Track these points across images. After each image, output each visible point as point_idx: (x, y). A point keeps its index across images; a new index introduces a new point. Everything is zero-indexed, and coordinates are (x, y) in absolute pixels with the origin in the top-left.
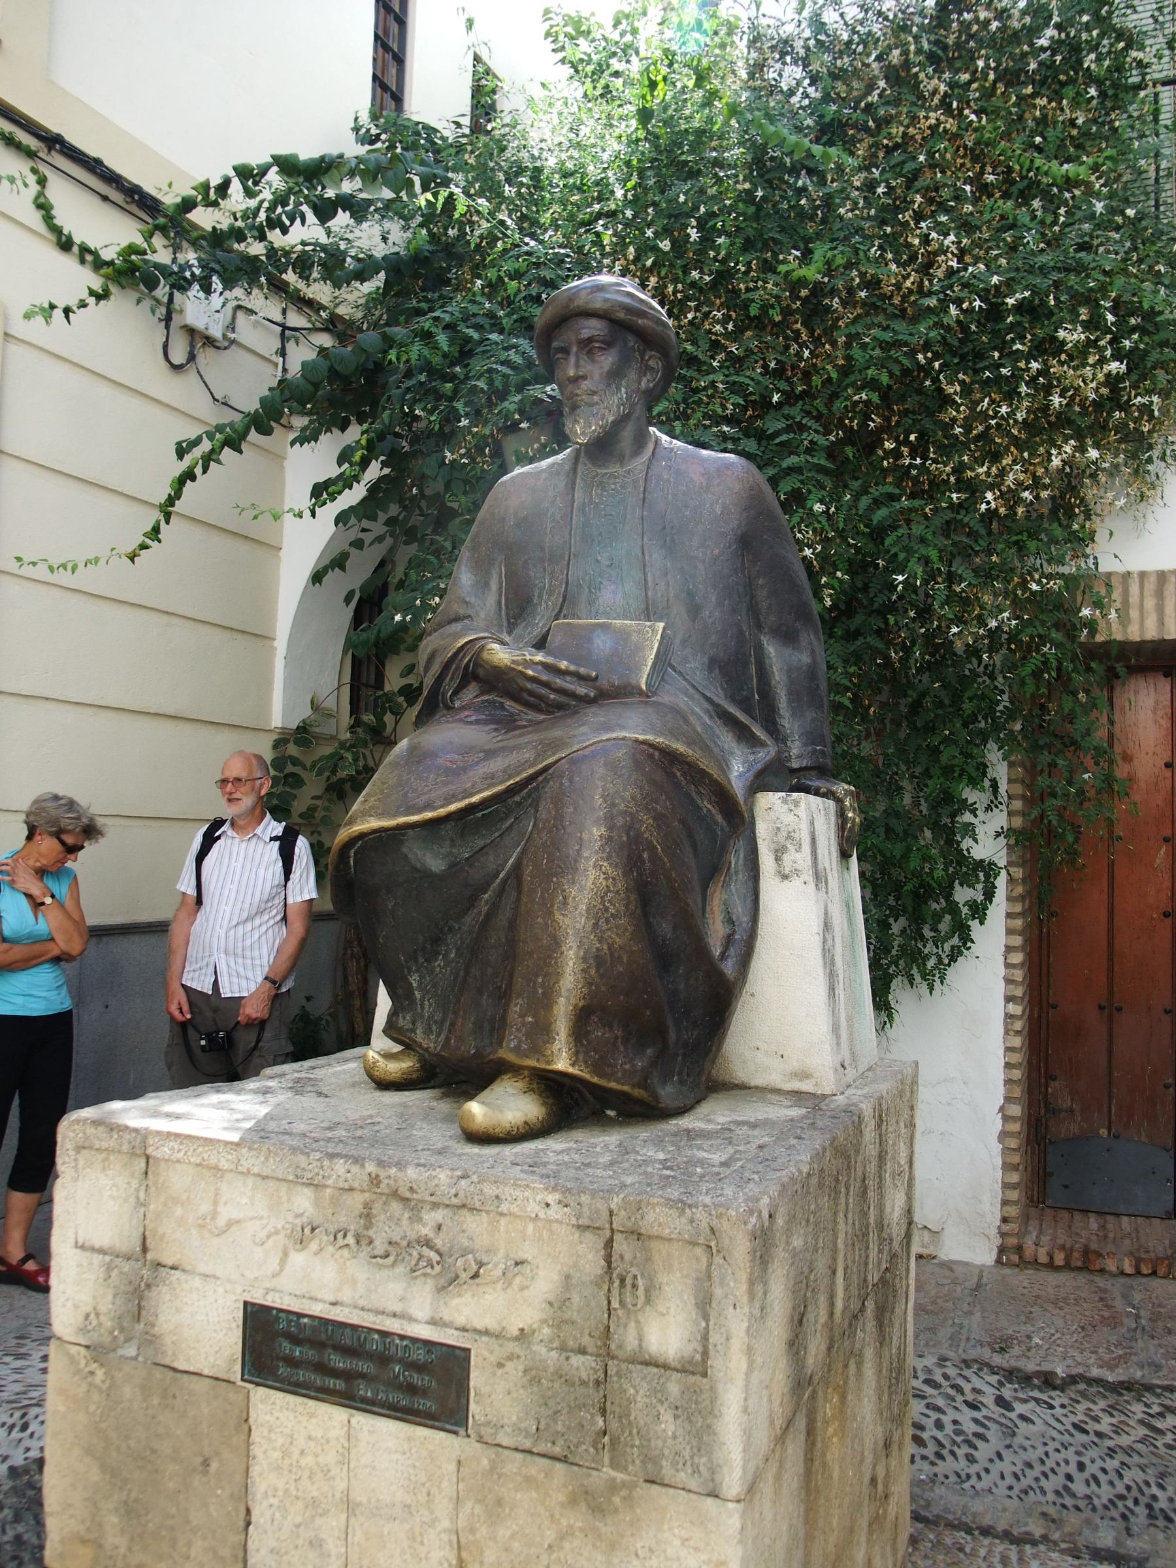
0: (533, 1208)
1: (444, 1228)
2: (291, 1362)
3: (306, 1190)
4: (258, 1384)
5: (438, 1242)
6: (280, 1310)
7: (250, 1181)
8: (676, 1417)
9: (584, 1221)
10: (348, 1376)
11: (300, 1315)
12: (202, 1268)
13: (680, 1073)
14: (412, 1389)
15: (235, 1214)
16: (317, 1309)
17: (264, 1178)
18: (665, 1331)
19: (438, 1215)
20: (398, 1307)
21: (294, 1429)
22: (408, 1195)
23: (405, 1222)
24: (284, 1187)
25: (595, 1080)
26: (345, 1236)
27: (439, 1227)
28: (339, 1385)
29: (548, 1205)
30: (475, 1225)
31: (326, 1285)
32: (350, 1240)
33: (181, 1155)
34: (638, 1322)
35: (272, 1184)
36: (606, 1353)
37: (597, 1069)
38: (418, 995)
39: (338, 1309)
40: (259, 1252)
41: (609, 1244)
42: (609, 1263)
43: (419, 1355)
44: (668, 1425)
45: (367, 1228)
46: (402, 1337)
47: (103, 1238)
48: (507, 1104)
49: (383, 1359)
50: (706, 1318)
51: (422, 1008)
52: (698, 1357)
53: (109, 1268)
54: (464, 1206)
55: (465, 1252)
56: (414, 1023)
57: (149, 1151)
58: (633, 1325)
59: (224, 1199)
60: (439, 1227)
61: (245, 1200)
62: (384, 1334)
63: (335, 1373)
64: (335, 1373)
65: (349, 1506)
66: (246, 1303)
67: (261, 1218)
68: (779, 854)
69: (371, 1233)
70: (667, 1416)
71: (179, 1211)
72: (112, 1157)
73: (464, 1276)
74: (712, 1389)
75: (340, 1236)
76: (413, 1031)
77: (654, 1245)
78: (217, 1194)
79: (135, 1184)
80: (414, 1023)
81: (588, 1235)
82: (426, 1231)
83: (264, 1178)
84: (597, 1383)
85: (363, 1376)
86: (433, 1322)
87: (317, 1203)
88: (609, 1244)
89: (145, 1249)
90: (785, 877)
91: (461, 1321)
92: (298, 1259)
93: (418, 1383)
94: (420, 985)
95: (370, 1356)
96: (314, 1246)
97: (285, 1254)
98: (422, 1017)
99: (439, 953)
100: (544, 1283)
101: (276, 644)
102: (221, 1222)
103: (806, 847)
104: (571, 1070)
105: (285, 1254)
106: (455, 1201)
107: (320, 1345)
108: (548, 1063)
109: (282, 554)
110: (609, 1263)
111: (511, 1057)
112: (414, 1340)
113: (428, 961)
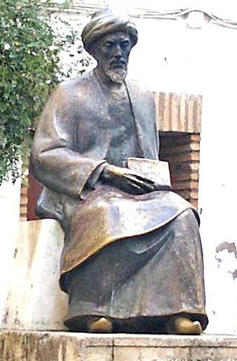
3: (170, 349)
5: (212, 358)
7: (152, 349)
17: (156, 347)
19: (212, 350)
22: (203, 345)
24: (163, 349)
33: (127, 344)
38: (113, 298)
51: (114, 301)
57: (115, 344)
59: (143, 355)
60: (212, 354)
61: (150, 355)
78: (141, 354)
80: (108, 310)
82: (208, 355)
83: (156, 347)
87: (174, 352)
98: (113, 306)
99: (125, 282)
113: (122, 284)
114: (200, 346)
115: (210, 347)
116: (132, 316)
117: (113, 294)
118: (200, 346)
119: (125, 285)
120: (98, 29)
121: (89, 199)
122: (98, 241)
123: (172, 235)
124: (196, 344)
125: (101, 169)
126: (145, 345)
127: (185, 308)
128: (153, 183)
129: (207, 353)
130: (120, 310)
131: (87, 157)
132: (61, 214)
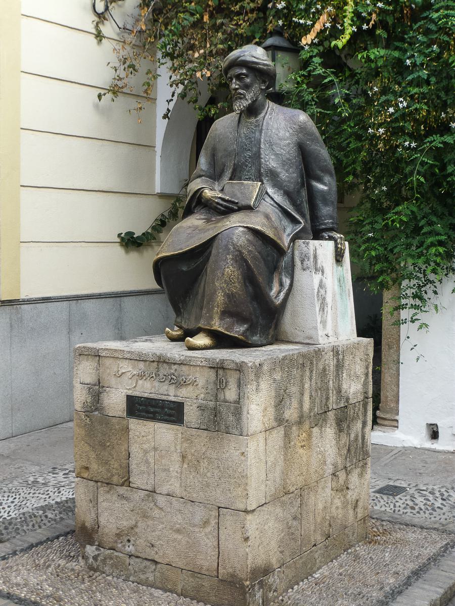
2: (139, 410)
5: (176, 374)
6: (136, 397)
7: (127, 361)
8: (233, 416)
9: (211, 366)
10: (154, 413)
11: (141, 398)
12: (115, 387)
13: (260, 334)
14: (170, 415)
15: (124, 371)
16: (146, 395)
17: (131, 359)
18: (231, 394)
19: (176, 367)
20: (166, 393)
21: (140, 428)
23: (168, 369)
24: (136, 362)
25: (226, 332)
28: (151, 415)
30: (184, 368)
31: (147, 389)
32: (154, 375)
33: (108, 355)
35: (133, 361)
36: (216, 400)
37: (226, 329)
39: (151, 395)
40: (130, 381)
41: (217, 372)
42: (217, 376)
43: (172, 406)
45: (158, 372)
46: (167, 401)
47: (88, 380)
48: (201, 340)
49: (163, 408)
51: (184, 314)
52: (238, 400)
53: (90, 389)
54: (182, 364)
56: (181, 320)
58: (223, 392)
62: (163, 400)
63: (151, 413)
64: (151, 413)
65: (155, 449)
66: (127, 395)
67: (130, 371)
68: (302, 261)
69: (159, 373)
70: (230, 415)
71: (108, 371)
72: (89, 357)
74: (241, 407)
76: (181, 322)
77: (227, 371)
79: (96, 364)
81: (212, 370)
83: (131, 359)
84: (214, 408)
85: (157, 413)
87: (145, 366)
88: (217, 372)
89: (99, 383)
90: (304, 270)
91: (181, 395)
92: (140, 382)
93: (172, 413)
95: (159, 407)
96: (145, 378)
97: (137, 381)
100: (201, 382)
101: (156, 149)
102: (120, 373)
103: (312, 259)
104: (220, 329)
105: (137, 381)
106: (179, 362)
107: (146, 406)
108: (211, 327)
109: (158, 101)
110: (217, 376)
111: (202, 326)
112: (171, 401)
114: (164, 362)
115: (175, 364)
117: (181, 307)
118: (164, 362)
119: (188, 299)
124: (162, 360)
126: (121, 357)
127: (202, 324)
129: (171, 369)
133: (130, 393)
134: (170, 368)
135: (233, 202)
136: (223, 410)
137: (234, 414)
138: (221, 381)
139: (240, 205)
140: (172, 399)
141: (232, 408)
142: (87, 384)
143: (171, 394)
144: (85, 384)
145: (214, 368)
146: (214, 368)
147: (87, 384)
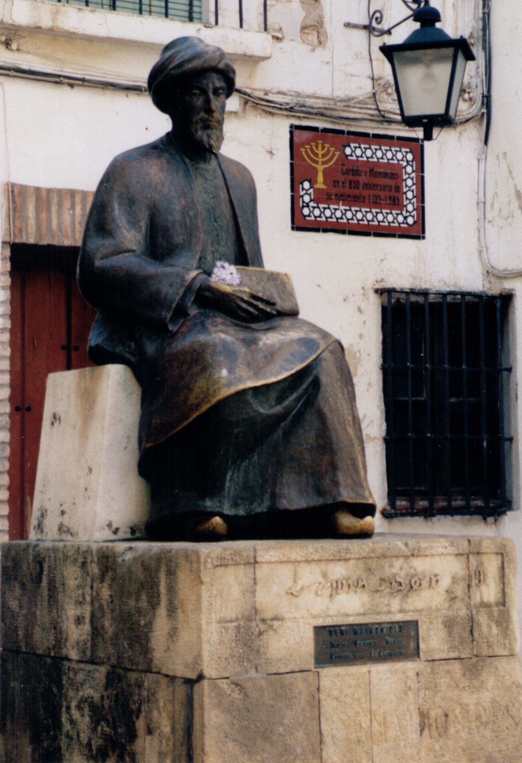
0: (440, 550)
1: (404, 568)
4: (323, 668)
8: (497, 626)
9: (461, 552)
16: (351, 620)
20: (385, 609)
26: (362, 581)
27: (401, 568)
29: (446, 547)
31: (351, 607)
34: (480, 590)
44: (495, 630)
50: (504, 583)
55: (413, 576)
57: (259, 559)
60: (401, 568)
73: (415, 587)
74: (508, 611)
75: (360, 581)
76: (221, 507)
81: (460, 557)
86: (401, 611)
94: (231, 477)
100: (445, 582)
116: (259, 510)
117: (228, 478)
120: (180, 66)
121: (184, 329)
122: (206, 396)
123: (316, 384)
125: (197, 284)
128: (274, 304)
130: (240, 502)
131: (172, 265)
132: (134, 356)
133: (320, 622)
134: (391, 566)
135: (268, 303)
136: (482, 618)
137: (498, 623)
138: (477, 573)
139: (278, 307)
140: (399, 617)
141: (496, 614)
142: (231, 621)
143: (394, 610)
144: (226, 622)
145: (461, 555)
146: (461, 555)
147: (231, 621)
